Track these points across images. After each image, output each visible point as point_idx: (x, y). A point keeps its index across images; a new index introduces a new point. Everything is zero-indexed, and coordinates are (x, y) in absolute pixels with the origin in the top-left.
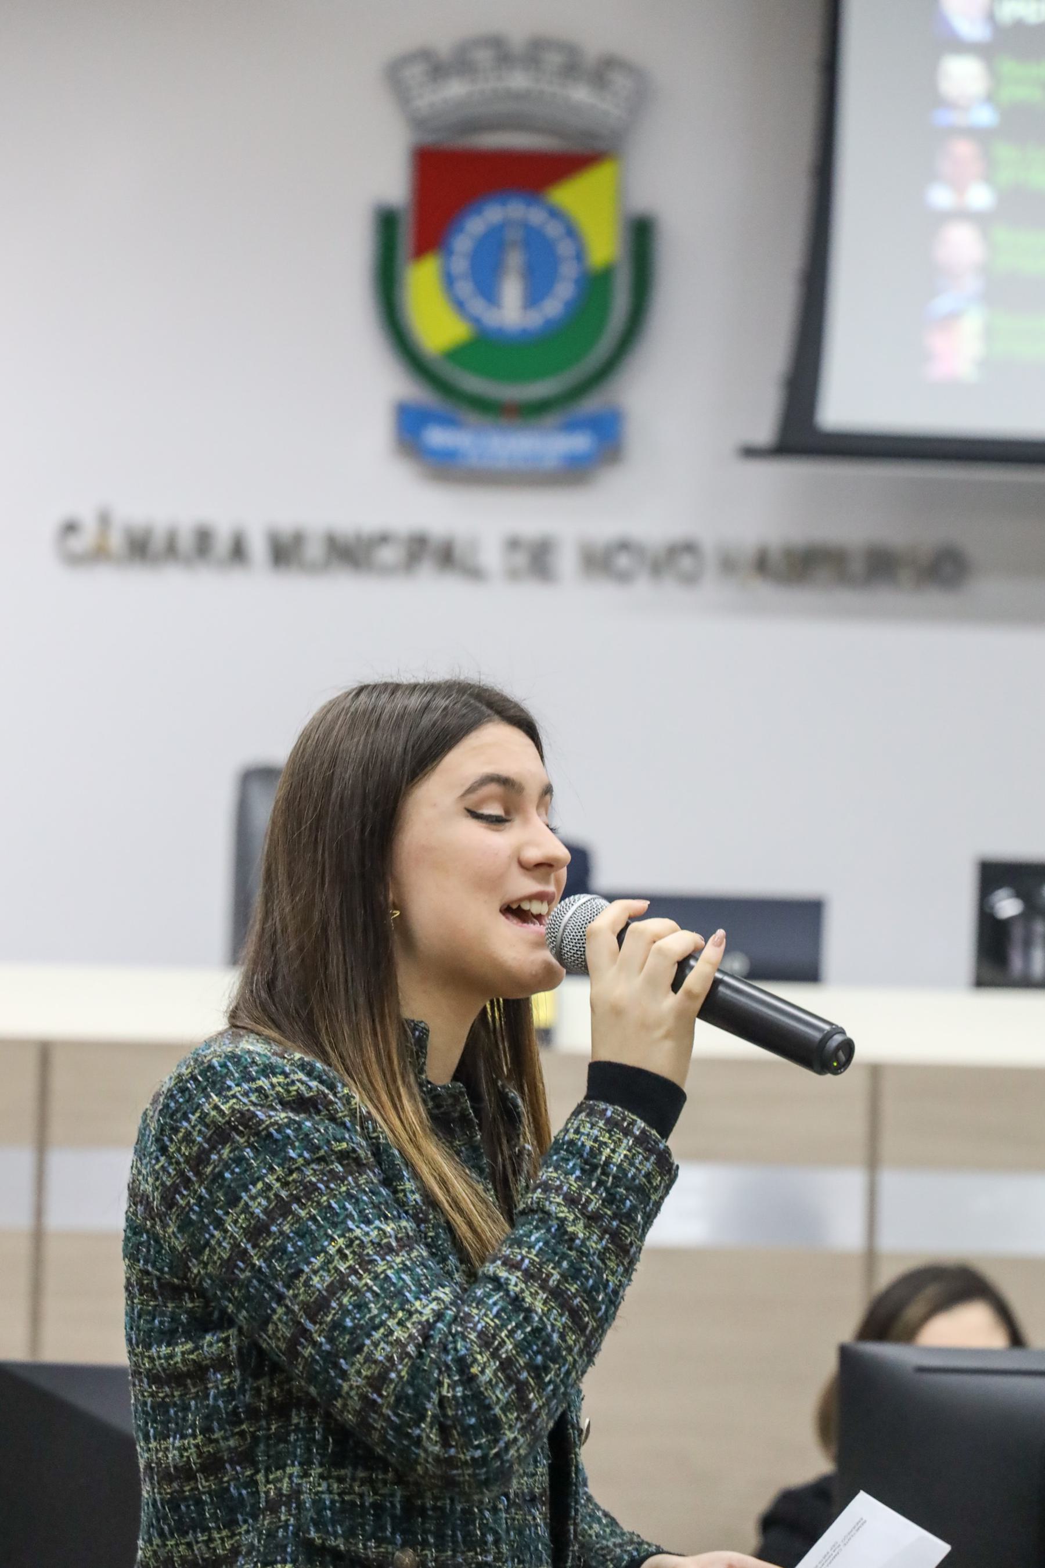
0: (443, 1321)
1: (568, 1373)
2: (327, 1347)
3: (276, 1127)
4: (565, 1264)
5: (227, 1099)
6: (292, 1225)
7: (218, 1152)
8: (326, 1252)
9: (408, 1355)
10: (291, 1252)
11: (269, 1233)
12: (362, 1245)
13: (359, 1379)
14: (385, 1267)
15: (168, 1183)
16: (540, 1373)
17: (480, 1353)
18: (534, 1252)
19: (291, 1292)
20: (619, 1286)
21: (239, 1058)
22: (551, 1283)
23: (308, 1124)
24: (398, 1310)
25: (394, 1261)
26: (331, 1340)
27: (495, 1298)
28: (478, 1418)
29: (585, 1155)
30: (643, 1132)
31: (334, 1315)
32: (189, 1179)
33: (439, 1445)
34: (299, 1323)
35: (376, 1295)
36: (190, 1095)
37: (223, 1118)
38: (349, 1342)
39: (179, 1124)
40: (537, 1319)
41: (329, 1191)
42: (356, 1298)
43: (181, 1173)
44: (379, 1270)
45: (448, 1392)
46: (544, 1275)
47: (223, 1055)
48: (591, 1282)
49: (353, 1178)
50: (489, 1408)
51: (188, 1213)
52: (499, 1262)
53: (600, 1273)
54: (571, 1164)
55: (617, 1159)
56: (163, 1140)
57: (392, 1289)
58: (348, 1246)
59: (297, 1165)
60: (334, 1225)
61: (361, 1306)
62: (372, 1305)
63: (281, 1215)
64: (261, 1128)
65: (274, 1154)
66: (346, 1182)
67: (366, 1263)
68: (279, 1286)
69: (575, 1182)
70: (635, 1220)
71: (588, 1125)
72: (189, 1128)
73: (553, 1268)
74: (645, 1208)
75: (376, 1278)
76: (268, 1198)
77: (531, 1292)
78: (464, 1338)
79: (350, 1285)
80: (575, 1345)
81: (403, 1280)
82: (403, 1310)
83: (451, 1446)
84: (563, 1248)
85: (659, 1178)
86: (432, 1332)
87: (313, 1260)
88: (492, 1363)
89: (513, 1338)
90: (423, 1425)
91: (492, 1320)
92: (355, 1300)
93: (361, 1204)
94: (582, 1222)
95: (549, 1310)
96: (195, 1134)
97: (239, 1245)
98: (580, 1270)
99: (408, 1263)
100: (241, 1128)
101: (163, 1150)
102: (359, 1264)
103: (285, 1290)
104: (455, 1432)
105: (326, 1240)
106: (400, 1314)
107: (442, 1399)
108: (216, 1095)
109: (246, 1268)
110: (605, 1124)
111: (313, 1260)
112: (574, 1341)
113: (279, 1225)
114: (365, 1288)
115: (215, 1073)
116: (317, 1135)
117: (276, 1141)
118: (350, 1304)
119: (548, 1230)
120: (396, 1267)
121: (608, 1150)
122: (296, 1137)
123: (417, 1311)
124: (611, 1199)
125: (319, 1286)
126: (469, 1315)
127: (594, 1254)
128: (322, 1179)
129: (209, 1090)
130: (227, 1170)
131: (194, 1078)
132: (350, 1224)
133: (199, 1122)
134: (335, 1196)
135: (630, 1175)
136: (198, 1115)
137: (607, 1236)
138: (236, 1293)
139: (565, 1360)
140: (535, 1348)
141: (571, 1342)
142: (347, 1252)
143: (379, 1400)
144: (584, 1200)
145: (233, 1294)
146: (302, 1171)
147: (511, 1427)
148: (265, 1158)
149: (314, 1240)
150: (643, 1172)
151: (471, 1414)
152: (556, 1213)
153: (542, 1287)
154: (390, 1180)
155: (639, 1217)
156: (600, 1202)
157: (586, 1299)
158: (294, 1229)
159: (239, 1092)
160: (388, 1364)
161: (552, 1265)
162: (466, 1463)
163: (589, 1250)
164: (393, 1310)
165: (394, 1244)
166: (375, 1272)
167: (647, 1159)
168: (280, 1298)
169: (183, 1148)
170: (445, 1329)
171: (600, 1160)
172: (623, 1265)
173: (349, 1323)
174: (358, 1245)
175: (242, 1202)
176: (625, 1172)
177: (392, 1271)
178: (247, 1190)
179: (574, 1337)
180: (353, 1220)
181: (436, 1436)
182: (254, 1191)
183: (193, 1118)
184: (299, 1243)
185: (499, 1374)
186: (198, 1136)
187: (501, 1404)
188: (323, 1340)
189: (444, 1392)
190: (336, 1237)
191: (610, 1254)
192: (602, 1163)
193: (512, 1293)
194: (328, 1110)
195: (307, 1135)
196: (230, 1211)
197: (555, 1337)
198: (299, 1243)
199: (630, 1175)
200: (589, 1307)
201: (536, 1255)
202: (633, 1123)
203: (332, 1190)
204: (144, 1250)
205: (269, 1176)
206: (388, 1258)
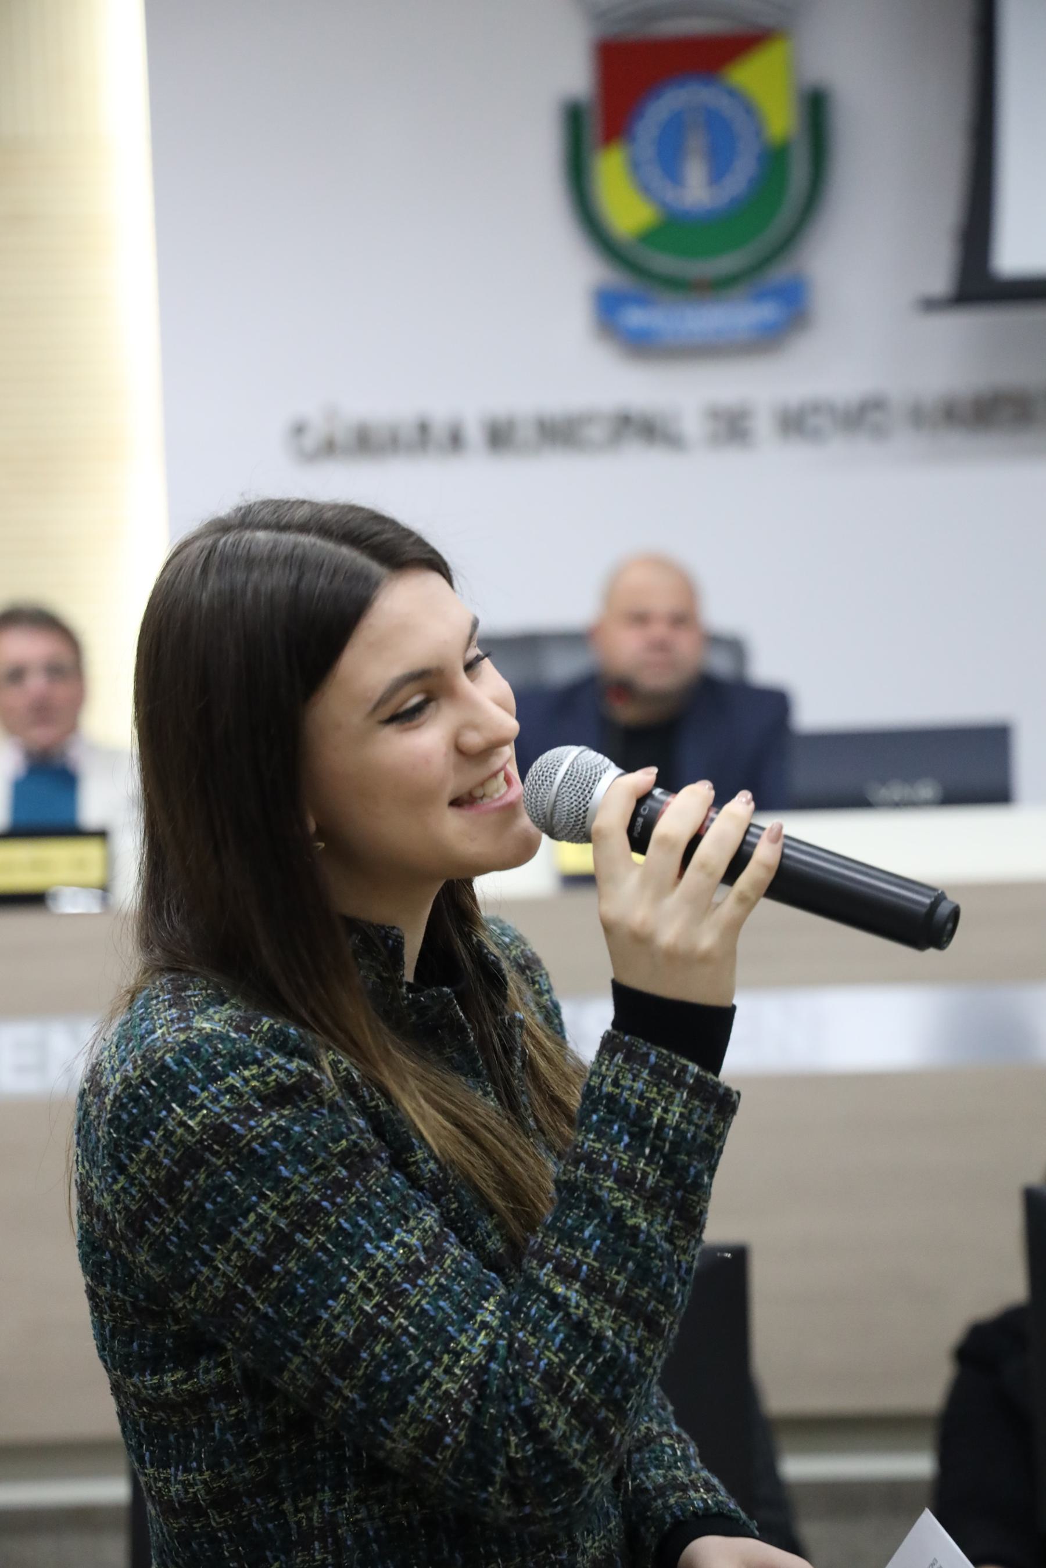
0: (496, 1359)
2: (361, 1405)
5: (194, 1111)
6: (298, 1260)
7: (192, 1178)
8: (347, 1292)
9: (464, 1415)
10: (303, 1295)
12: (388, 1274)
13: (406, 1441)
14: (418, 1297)
15: (134, 1208)
17: (548, 1402)
18: (591, 1253)
19: (308, 1342)
21: (198, 1048)
22: (618, 1291)
24: (442, 1353)
25: (427, 1285)
26: (366, 1397)
27: (555, 1322)
29: (631, 1115)
31: (367, 1367)
32: (160, 1206)
34: (323, 1377)
35: (414, 1338)
36: (146, 1105)
37: (193, 1137)
38: (388, 1399)
39: (138, 1143)
40: (608, 1347)
41: (335, 1208)
42: (390, 1345)
43: (147, 1197)
45: (517, 1453)
46: (608, 1285)
47: (177, 1048)
49: (361, 1180)
50: (566, 1462)
51: (164, 1244)
52: (550, 1266)
54: (616, 1127)
55: (673, 1119)
56: (119, 1158)
59: (293, 1185)
60: (350, 1251)
61: (398, 1355)
62: (411, 1352)
63: (283, 1251)
65: (263, 1175)
66: (354, 1190)
67: (394, 1295)
68: (293, 1334)
69: (624, 1152)
71: (630, 1076)
72: (153, 1148)
73: (618, 1273)
75: (410, 1314)
76: (264, 1232)
77: (596, 1310)
78: (526, 1382)
79: (380, 1329)
81: (441, 1308)
82: (448, 1352)
83: (525, 1505)
84: (625, 1246)
86: (486, 1377)
87: (330, 1302)
88: (563, 1411)
89: (583, 1374)
90: (490, 1489)
91: (555, 1354)
92: (390, 1348)
93: (377, 1213)
94: (641, 1205)
96: (161, 1155)
97: (236, 1287)
98: (649, 1269)
99: (443, 1280)
100: (216, 1147)
101: (122, 1169)
102: (386, 1299)
103: (300, 1340)
104: (529, 1493)
105: (344, 1275)
106: (446, 1358)
107: (511, 1462)
108: (180, 1106)
109: (248, 1311)
110: (650, 1074)
111: (330, 1302)
113: (283, 1262)
114: (400, 1330)
115: (172, 1075)
116: (309, 1140)
117: (262, 1158)
118: (385, 1353)
119: (603, 1219)
121: (659, 1109)
122: (286, 1149)
123: (464, 1349)
124: (670, 1168)
125: (343, 1333)
126: (524, 1344)
128: (325, 1193)
129: (168, 1098)
130: (207, 1200)
131: (146, 1083)
133: (165, 1142)
134: (344, 1212)
136: (161, 1133)
137: (672, 1212)
138: (237, 1335)
140: (611, 1379)
142: (371, 1286)
143: (433, 1463)
144: (639, 1176)
145: (233, 1334)
146: (300, 1189)
148: (252, 1180)
149: (330, 1275)
150: (704, 1127)
152: (610, 1202)
153: (607, 1301)
154: (400, 1161)
158: (301, 1264)
159: (207, 1098)
160: (439, 1424)
161: (614, 1270)
162: (545, 1519)
164: (436, 1354)
166: (408, 1307)
167: (706, 1111)
168: (296, 1349)
169: (148, 1170)
170: (501, 1370)
171: (652, 1123)
173: (386, 1378)
174: (382, 1274)
175: (233, 1238)
176: (683, 1133)
177: (427, 1299)
178: (237, 1224)
180: (371, 1240)
182: (246, 1225)
183: (157, 1135)
184: (311, 1282)
185: (573, 1421)
186: (165, 1157)
188: (355, 1396)
189: (512, 1454)
190: (355, 1270)
191: (678, 1231)
192: (654, 1126)
193: (574, 1317)
194: (316, 1094)
195: (299, 1144)
196: (219, 1246)
198: (311, 1282)
199: (689, 1135)
201: (595, 1260)
202: (684, 1069)
203: (339, 1206)
204: (109, 1271)
205: (263, 1205)
206: (420, 1282)
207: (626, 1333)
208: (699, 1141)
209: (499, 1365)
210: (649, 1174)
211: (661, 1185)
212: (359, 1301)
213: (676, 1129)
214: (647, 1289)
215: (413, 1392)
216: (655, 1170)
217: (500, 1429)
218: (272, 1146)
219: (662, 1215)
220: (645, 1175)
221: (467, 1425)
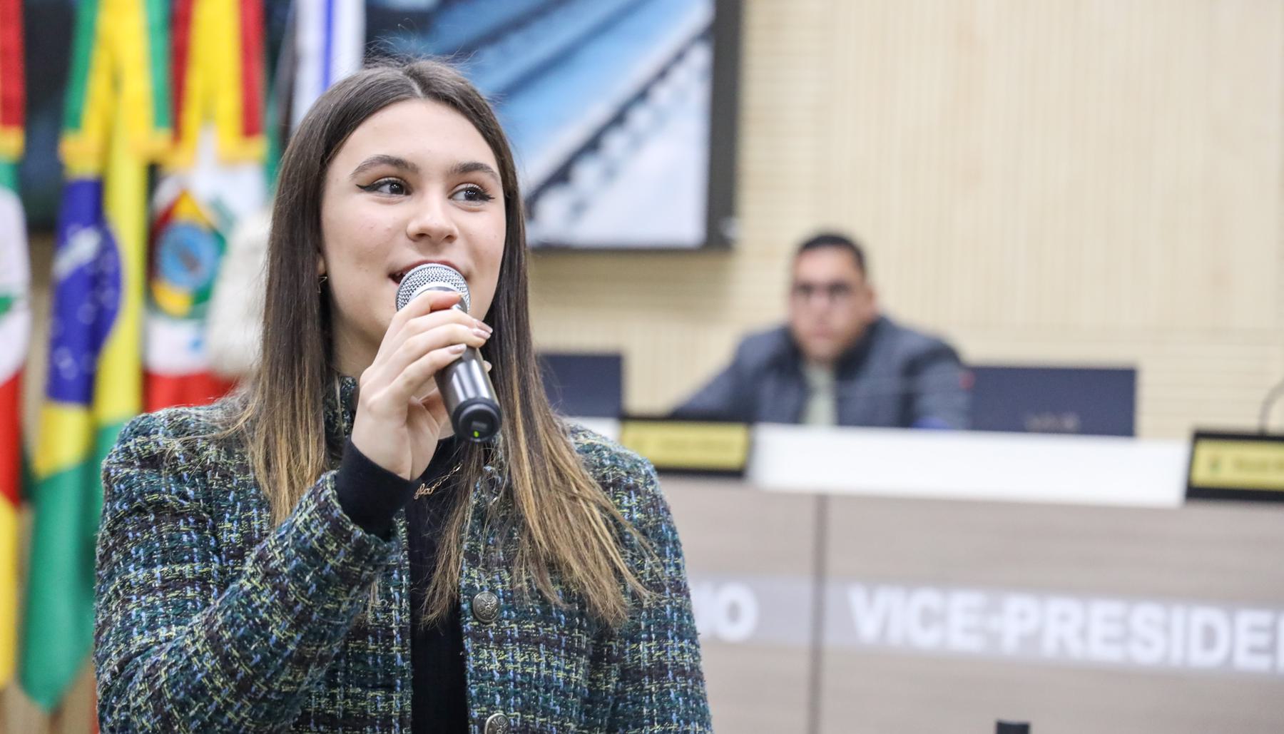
1: (219, 712)
4: (229, 612)
16: (183, 706)
20: (285, 640)
22: (215, 628)
30: (327, 499)
48: (242, 630)
70: (302, 581)
85: (335, 544)
88: (148, 693)
98: (234, 620)
112: (223, 684)
127: (261, 607)
135: (303, 537)
137: (277, 593)
139: (211, 700)
140: (181, 684)
141: (218, 684)
155: (308, 578)
156: (283, 560)
163: (251, 602)
167: (322, 524)
187: (146, 729)
191: (276, 608)
197: (199, 675)
199: (303, 537)
200: (240, 654)
207: (205, 658)
208: (308, 544)
210: (276, 558)
213: (298, 529)
214: (229, 633)
216: (281, 558)
220: (273, 558)
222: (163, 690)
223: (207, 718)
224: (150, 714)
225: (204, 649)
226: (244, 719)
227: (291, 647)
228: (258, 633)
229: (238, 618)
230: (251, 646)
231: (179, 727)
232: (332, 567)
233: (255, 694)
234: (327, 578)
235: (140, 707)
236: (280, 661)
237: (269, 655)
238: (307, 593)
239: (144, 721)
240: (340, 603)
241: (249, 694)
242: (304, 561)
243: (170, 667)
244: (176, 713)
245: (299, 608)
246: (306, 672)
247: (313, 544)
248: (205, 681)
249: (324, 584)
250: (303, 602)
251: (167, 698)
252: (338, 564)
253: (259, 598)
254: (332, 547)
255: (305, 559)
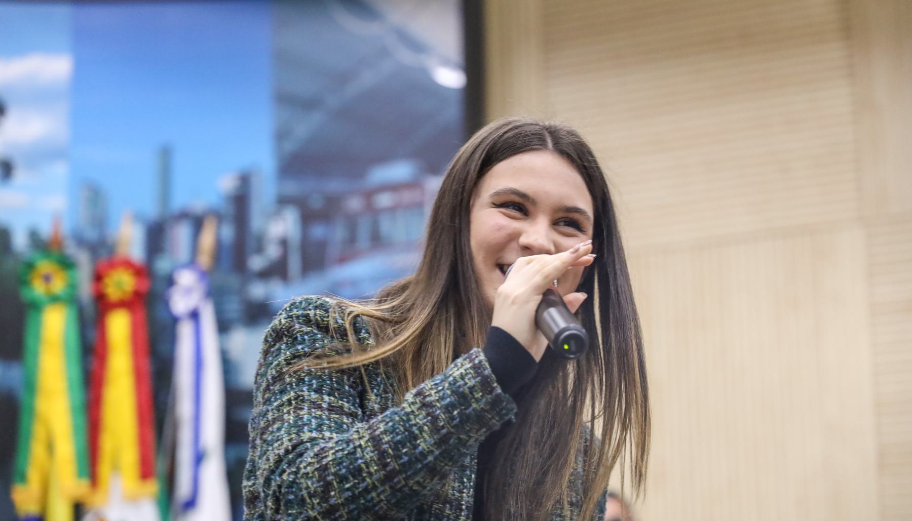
1: (367, 491)
3: (301, 333)
6: (280, 386)
11: (269, 390)
16: (342, 479)
17: (311, 458)
20: (428, 452)
23: (319, 336)
24: (294, 433)
28: (296, 496)
30: (480, 362)
33: (273, 511)
44: (301, 413)
53: (416, 438)
57: (300, 423)
58: (295, 399)
59: (298, 354)
61: (279, 429)
64: (294, 333)
69: (432, 386)
70: (451, 413)
74: (465, 409)
80: (376, 474)
81: (311, 421)
85: (481, 394)
89: (335, 455)
95: (366, 447)
120: (313, 415)
127: (415, 425)
132: (305, 389)
134: (311, 375)
135: (458, 384)
139: (364, 480)
141: (372, 470)
142: (293, 402)
147: (313, 508)
150: (468, 385)
151: (292, 493)
155: (455, 412)
156: (437, 398)
157: (393, 447)
163: (409, 420)
165: (325, 405)
167: (474, 378)
172: (434, 439)
174: (301, 400)
179: (375, 468)
181: (273, 504)
185: (316, 473)
187: (310, 490)
197: (360, 461)
199: (458, 384)
206: (313, 410)
207: (366, 451)
208: (461, 389)
209: (311, 444)
211: (434, 403)
212: (285, 406)
214: (389, 438)
215: (272, 445)
216: (436, 396)
217: (286, 465)
218: (303, 337)
219: (424, 416)
220: (430, 395)
221: (277, 459)
222: (328, 466)
223: (357, 492)
224: (314, 479)
225: (367, 445)
226: (382, 500)
227: (430, 458)
228: (410, 442)
229: (398, 428)
230: (403, 449)
231: (335, 494)
232: (474, 410)
233: (395, 484)
234: (468, 417)
235: (307, 474)
236: (420, 466)
237: (414, 459)
238: (452, 422)
239: (309, 483)
240: (470, 437)
241: (391, 483)
242: (455, 400)
243: (337, 451)
244: (335, 483)
245: (444, 431)
246: (432, 480)
247: (465, 390)
248: (363, 466)
249: (465, 419)
250: (448, 428)
251: (331, 472)
252: (478, 408)
253: (415, 419)
254: (478, 395)
255: (457, 399)
